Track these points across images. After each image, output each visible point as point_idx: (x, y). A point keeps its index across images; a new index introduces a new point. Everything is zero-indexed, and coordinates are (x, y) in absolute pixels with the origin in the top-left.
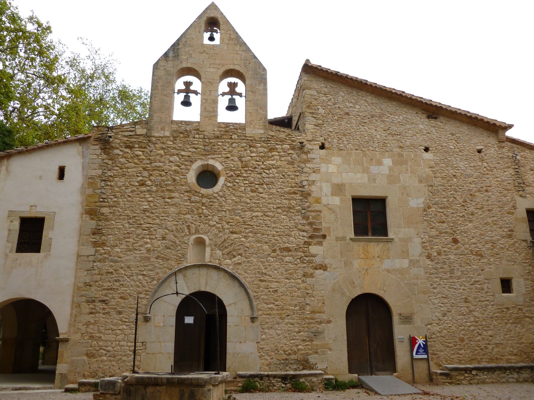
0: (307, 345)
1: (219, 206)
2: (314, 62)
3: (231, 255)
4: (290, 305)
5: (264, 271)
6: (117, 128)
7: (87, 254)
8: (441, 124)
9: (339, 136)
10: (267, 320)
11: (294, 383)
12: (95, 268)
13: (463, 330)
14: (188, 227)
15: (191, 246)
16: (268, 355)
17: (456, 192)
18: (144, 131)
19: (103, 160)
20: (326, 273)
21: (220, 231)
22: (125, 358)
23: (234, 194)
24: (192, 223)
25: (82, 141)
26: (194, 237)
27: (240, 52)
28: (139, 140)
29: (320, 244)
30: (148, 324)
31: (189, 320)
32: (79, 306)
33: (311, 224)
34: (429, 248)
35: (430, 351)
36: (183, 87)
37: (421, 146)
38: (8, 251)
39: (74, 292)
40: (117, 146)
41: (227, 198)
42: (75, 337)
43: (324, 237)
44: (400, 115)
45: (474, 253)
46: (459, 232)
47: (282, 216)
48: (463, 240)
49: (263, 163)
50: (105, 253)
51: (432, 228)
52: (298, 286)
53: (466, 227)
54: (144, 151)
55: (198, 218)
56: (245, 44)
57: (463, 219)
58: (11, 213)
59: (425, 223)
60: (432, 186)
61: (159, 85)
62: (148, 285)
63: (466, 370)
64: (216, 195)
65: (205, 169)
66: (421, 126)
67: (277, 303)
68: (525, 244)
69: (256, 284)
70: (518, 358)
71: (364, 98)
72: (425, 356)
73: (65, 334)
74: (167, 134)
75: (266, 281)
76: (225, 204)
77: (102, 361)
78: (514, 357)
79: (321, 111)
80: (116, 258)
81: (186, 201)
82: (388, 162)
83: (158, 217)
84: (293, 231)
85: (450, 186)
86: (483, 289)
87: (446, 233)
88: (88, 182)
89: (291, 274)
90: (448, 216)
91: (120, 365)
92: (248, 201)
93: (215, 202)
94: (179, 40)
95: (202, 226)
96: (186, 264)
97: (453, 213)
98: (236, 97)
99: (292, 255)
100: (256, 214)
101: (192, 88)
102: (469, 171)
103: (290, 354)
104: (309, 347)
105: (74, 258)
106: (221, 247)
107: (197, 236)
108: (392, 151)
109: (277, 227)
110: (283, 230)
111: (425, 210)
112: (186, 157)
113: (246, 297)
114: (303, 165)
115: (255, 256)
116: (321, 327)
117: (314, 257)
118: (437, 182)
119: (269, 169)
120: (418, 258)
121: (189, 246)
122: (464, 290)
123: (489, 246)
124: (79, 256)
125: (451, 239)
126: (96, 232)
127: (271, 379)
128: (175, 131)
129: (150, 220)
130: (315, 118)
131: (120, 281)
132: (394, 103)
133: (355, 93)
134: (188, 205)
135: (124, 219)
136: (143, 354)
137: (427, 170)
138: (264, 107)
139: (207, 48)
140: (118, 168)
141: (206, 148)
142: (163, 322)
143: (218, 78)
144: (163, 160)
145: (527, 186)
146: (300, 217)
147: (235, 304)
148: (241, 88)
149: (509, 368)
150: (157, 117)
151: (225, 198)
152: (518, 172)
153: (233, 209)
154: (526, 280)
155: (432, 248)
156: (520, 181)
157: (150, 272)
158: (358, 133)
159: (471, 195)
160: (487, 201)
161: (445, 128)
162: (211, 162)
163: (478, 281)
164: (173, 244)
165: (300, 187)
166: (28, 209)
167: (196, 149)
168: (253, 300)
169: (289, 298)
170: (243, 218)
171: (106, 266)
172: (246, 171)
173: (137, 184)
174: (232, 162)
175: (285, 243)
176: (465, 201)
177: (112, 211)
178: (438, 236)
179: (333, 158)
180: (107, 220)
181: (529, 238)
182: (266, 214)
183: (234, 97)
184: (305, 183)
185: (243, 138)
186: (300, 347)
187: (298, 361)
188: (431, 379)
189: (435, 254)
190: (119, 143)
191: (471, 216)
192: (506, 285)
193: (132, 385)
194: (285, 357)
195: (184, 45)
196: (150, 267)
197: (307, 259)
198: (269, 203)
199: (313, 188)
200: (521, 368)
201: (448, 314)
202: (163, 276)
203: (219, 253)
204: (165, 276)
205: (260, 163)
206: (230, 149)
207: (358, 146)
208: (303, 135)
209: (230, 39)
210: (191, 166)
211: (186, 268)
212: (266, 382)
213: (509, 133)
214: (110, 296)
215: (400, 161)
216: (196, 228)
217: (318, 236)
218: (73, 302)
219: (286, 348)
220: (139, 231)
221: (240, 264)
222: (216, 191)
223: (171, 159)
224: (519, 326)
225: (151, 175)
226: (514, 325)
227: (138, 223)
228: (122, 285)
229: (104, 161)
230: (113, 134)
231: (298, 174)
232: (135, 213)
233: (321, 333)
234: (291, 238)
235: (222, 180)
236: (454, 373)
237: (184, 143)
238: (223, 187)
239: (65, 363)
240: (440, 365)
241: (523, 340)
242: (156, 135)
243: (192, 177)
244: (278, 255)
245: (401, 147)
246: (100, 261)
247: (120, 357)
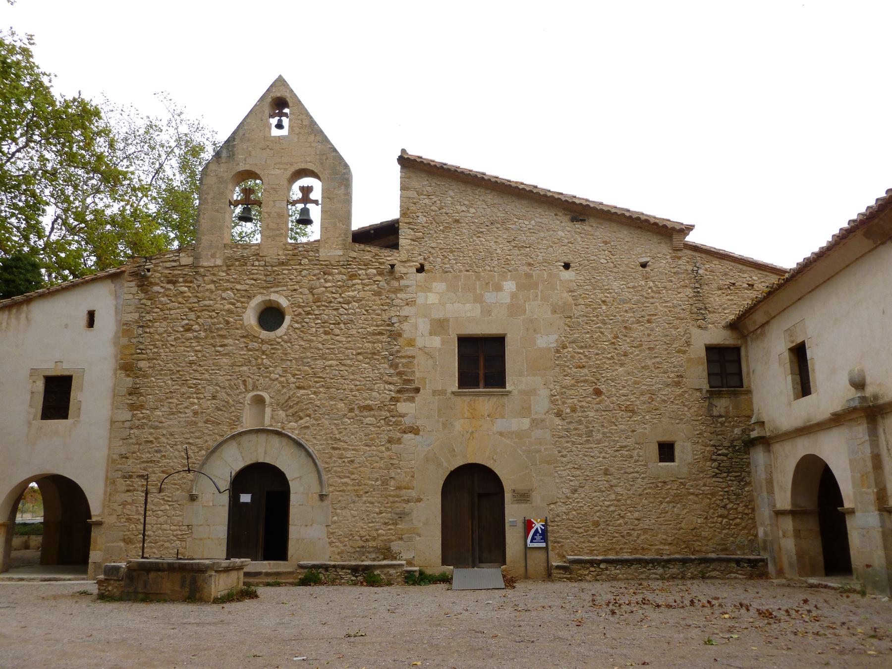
0: (389, 530)
2: (413, 151)
3: (297, 417)
4: (369, 479)
5: (338, 436)
7: (123, 419)
8: (590, 229)
11: (366, 576)
12: (132, 436)
13: (599, 511)
14: (244, 381)
15: (247, 407)
16: (341, 542)
17: (605, 324)
18: (190, 261)
19: (140, 300)
21: (283, 387)
22: (167, 544)
23: (302, 338)
25: (114, 277)
26: (251, 394)
27: (314, 145)
29: (412, 400)
30: (195, 503)
31: (246, 498)
32: (113, 483)
33: (400, 374)
34: (560, 402)
37: (559, 261)
38: (32, 417)
39: (108, 465)
40: (157, 281)
42: (110, 520)
43: (417, 390)
44: (531, 219)
45: (623, 408)
46: (603, 380)
47: (364, 365)
48: (609, 391)
50: (144, 418)
52: (380, 455)
53: (614, 373)
56: (322, 132)
58: (33, 372)
61: (209, 197)
63: (592, 563)
64: (280, 340)
65: (268, 305)
66: (561, 233)
67: (353, 477)
68: (698, 394)
70: (672, 548)
72: (544, 545)
73: (99, 516)
74: (219, 262)
75: (339, 449)
76: (290, 351)
78: (667, 547)
79: (422, 219)
80: (157, 423)
81: (242, 349)
82: (510, 286)
83: (207, 370)
85: (597, 316)
86: (631, 457)
87: (585, 381)
88: (123, 330)
89: (372, 439)
90: (590, 358)
92: (320, 346)
94: (234, 133)
95: (261, 380)
97: (597, 354)
100: (330, 362)
102: (626, 295)
103: (367, 540)
105: (107, 425)
106: (285, 406)
107: (255, 393)
108: (517, 270)
109: (356, 380)
111: (558, 351)
113: (314, 469)
116: (408, 507)
118: (577, 311)
119: (348, 303)
120: (544, 416)
122: (604, 458)
123: (645, 398)
124: (113, 422)
125: (591, 389)
126: (133, 391)
127: (338, 570)
128: (229, 258)
129: (197, 375)
130: (413, 229)
132: (524, 202)
133: (469, 191)
135: (165, 375)
137: (565, 295)
138: (347, 217)
139: (272, 141)
141: (270, 278)
143: (286, 183)
144: (213, 296)
145: (710, 312)
146: (386, 366)
147: (300, 477)
149: (652, 561)
152: (698, 292)
153: (301, 358)
154: (694, 443)
155: (564, 403)
156: (700, 305)
158: (470, 248)
159: (626, 328)
160: (649, 335)
161: (598, 233)
162: (274, 297)
163: (625, 447)
165: (388, 325)
166: (52, 365)
167: (255, 280)
168: (323, 473)
169: (368, 471)
171: (145, 434)
172: (318, 307)
173: (182, 329)
175: (365, 399)
176: (616, 337)
177: (151, 365)
178: (574, 386)
179: (434, 284)
180: (145, 376)
181: (706, 386)
182: (343, 362)
184: (394, 320)
186: (380, 531)
187: (377, 550)
188: (549, 575)
189: (568, 410)
190: (159, 278)
192: (666, 451)
193: (134, 570)
194: (361, 543)
195: (242, 140)
197: (394, 420)
198: (347, 348)
199: (406, 326)
200: (668, 561)
201: (580, 490)
202: (212, 444)
203: (282, 414)
204: (216, 444)
206: (299, 278)
207: (471, 266)
209: (302, 127)
210: (248, 303)
211: (241, 434)
212: (332, 574)
213: (691, 238)
214: (150, 470)
215: (527, 284)
216: (254, 383)
217: (409, 389)
218: (107, 477)
219: (363, 533)
221: (307, 427)
223: (224, 295)
224: (679, 505)
225: (198, 317)
226: (671, 505)
228: (164, 456)
231: (386, 308)
233: (409, 514)
235: (288, 320)
236: (574, 566)
237: (241, 273)
238: (288, 329)
239: (100, 550)
240: (564, 557)
241: (683, 525)
242: (205, 264)
243: (250, 318)
244: (356, 416)
245: (530, 264)
246: (137, 427)
247: (162, 543)
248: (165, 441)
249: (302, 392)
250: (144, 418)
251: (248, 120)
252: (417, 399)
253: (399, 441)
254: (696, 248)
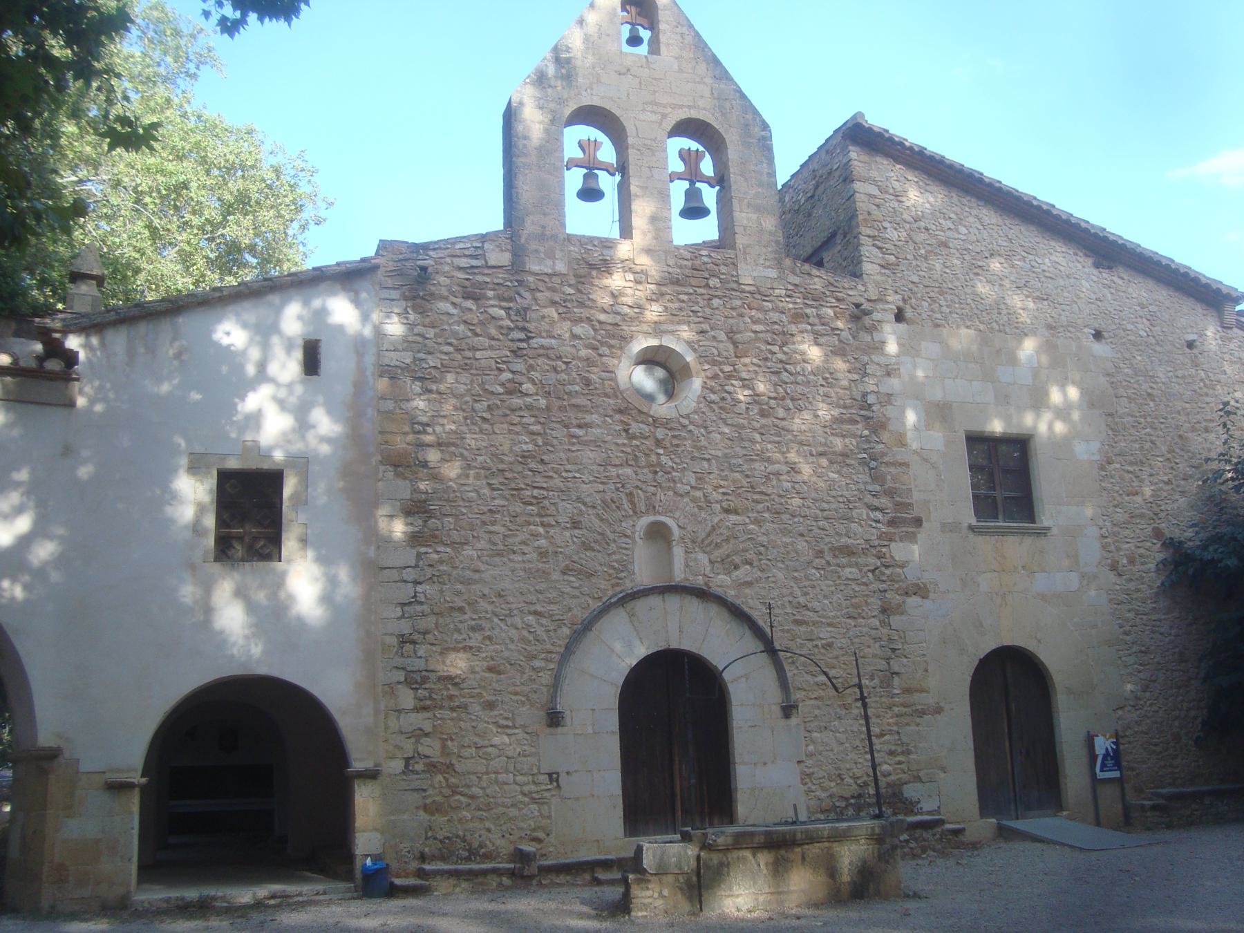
0: (899, 763)
1: (695, 447)
2: (876, 119)
5: (802, 600)
6: (440, 248)
8: (1120, 282)
9: (932, 294)
10: (817, 712)
20: (927, 603)
21: (700, 508)
22: (513, 812)
24: (637, 487)
28: (496, 281)
29: (911, 537)
33: (890, 493)
34: (1112, 548)
35: (1124, 764)
36: (579, 154)
40: (444, 292)
41: (711, 429)
43: (918, 522)
46: (1163, 515)
47: (831, 475)
49: (781, 347)
50: (441, 562)
51: (1115, 506)
53: (1175, 506)
54: (510, 308)
55: (650, 476)
57: (1169, 487)
59: (1105, 494)
60: (1111, 415)
62: (550, 637)
69: (788, 631)
71: (974, 212)
72: (1116, 774)
74: (561, 267)
77: (460, 820)
84: (855, 507)
91: (504, 828)
93: (685, 439)
95: (661, 496)
96: (628, 586)
98: (703, 187)
99: (857, 564)
104: (903, 766)
106: (705, 544)
107: (651, 518)
110: (834, 506)
111: (1102, 468)
112: (609, 327)
114: (866, 358)
115: (780, 565)
117: (902, 567)
121: (634, 542)
131: (483, 629)
132: (1032, 228)
134: (624, 445)
136: (554, 800)
140: (451, 349)
142: (593, 725)
147: (747, 676)
150: (533, 223)
151: (706, 428)
153: (726, 456)
155: (1118, 549)
157: (552, 607)
159: (1180, 436)
164: (599, 537)
170: (747, 476)
173: (501, 390)
174: (715, 344)
179: (924, 344)
183: (698, 185)
185: (734, 286)
189: (1125, 561)
191: (1182, 482)
194: (854, 789)
196: (552, 595)
197: (888, 572)
202: (580, 614)
203: (703, 558)
205: (776, 349)
210: (621, 348)
216: (647, 498)
217: (904, 520)
219: (858, 773)
220: (517, 507)
221: (749, 584)
222: (684, 412)
223: (578, 330)
225: (531, 368)
227: (513, 485)
228: (490, 638)
229: (416, 331)
230: (431, 262)
232: (502, 461)
234: (853, 525)
238: (699, 403)
244: (828, 563)
247: (501, 810)
248: (490, 608)
249: (733, 518)
250: (441, 562)
253: (900, 610)
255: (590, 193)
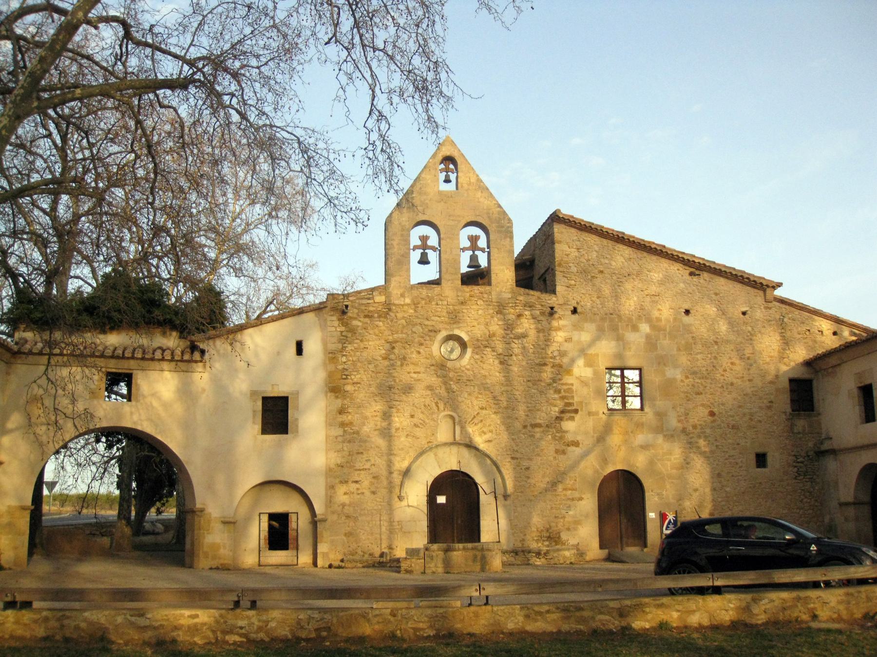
2: (566, 211)
5: (516, 448)
12: (345, 449)
19: (342, 332)
29: (572, 419)
31: (441, 499)
33: (563, 398)
36: (419, 243)
40: (355, 316)
50: (354, 433)
56: (487, 189)
101: (430, 243)
126: (341, 411)
128: (416, 297)
148: (482, 243)
181: (789, 410)
183: (476, 253)
192: (761, 460)
208: (554, 299)
213: (778, 292)
223: (414, 330)
242: (397, 302)
249: (484, 412)
250: (354, 433)
251: (423, 175)
252: (576, 419)
253: (564, 452)
254: (782, 301)
255: (424, 261)
